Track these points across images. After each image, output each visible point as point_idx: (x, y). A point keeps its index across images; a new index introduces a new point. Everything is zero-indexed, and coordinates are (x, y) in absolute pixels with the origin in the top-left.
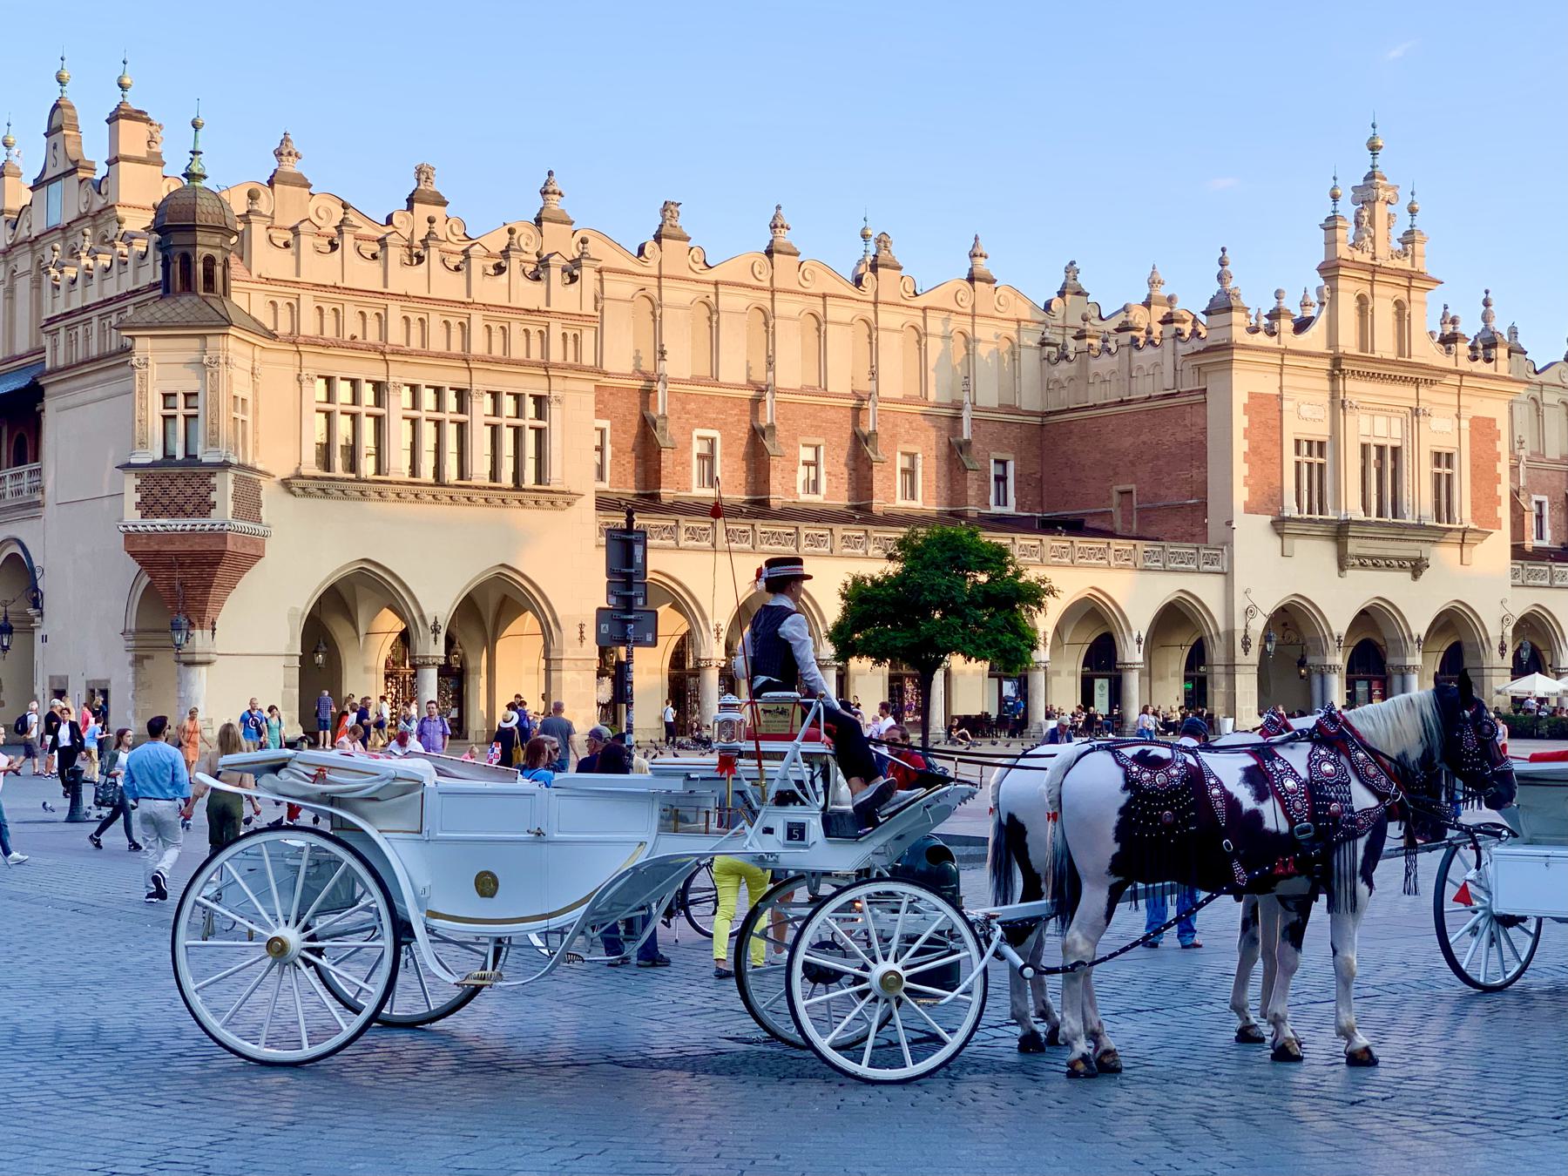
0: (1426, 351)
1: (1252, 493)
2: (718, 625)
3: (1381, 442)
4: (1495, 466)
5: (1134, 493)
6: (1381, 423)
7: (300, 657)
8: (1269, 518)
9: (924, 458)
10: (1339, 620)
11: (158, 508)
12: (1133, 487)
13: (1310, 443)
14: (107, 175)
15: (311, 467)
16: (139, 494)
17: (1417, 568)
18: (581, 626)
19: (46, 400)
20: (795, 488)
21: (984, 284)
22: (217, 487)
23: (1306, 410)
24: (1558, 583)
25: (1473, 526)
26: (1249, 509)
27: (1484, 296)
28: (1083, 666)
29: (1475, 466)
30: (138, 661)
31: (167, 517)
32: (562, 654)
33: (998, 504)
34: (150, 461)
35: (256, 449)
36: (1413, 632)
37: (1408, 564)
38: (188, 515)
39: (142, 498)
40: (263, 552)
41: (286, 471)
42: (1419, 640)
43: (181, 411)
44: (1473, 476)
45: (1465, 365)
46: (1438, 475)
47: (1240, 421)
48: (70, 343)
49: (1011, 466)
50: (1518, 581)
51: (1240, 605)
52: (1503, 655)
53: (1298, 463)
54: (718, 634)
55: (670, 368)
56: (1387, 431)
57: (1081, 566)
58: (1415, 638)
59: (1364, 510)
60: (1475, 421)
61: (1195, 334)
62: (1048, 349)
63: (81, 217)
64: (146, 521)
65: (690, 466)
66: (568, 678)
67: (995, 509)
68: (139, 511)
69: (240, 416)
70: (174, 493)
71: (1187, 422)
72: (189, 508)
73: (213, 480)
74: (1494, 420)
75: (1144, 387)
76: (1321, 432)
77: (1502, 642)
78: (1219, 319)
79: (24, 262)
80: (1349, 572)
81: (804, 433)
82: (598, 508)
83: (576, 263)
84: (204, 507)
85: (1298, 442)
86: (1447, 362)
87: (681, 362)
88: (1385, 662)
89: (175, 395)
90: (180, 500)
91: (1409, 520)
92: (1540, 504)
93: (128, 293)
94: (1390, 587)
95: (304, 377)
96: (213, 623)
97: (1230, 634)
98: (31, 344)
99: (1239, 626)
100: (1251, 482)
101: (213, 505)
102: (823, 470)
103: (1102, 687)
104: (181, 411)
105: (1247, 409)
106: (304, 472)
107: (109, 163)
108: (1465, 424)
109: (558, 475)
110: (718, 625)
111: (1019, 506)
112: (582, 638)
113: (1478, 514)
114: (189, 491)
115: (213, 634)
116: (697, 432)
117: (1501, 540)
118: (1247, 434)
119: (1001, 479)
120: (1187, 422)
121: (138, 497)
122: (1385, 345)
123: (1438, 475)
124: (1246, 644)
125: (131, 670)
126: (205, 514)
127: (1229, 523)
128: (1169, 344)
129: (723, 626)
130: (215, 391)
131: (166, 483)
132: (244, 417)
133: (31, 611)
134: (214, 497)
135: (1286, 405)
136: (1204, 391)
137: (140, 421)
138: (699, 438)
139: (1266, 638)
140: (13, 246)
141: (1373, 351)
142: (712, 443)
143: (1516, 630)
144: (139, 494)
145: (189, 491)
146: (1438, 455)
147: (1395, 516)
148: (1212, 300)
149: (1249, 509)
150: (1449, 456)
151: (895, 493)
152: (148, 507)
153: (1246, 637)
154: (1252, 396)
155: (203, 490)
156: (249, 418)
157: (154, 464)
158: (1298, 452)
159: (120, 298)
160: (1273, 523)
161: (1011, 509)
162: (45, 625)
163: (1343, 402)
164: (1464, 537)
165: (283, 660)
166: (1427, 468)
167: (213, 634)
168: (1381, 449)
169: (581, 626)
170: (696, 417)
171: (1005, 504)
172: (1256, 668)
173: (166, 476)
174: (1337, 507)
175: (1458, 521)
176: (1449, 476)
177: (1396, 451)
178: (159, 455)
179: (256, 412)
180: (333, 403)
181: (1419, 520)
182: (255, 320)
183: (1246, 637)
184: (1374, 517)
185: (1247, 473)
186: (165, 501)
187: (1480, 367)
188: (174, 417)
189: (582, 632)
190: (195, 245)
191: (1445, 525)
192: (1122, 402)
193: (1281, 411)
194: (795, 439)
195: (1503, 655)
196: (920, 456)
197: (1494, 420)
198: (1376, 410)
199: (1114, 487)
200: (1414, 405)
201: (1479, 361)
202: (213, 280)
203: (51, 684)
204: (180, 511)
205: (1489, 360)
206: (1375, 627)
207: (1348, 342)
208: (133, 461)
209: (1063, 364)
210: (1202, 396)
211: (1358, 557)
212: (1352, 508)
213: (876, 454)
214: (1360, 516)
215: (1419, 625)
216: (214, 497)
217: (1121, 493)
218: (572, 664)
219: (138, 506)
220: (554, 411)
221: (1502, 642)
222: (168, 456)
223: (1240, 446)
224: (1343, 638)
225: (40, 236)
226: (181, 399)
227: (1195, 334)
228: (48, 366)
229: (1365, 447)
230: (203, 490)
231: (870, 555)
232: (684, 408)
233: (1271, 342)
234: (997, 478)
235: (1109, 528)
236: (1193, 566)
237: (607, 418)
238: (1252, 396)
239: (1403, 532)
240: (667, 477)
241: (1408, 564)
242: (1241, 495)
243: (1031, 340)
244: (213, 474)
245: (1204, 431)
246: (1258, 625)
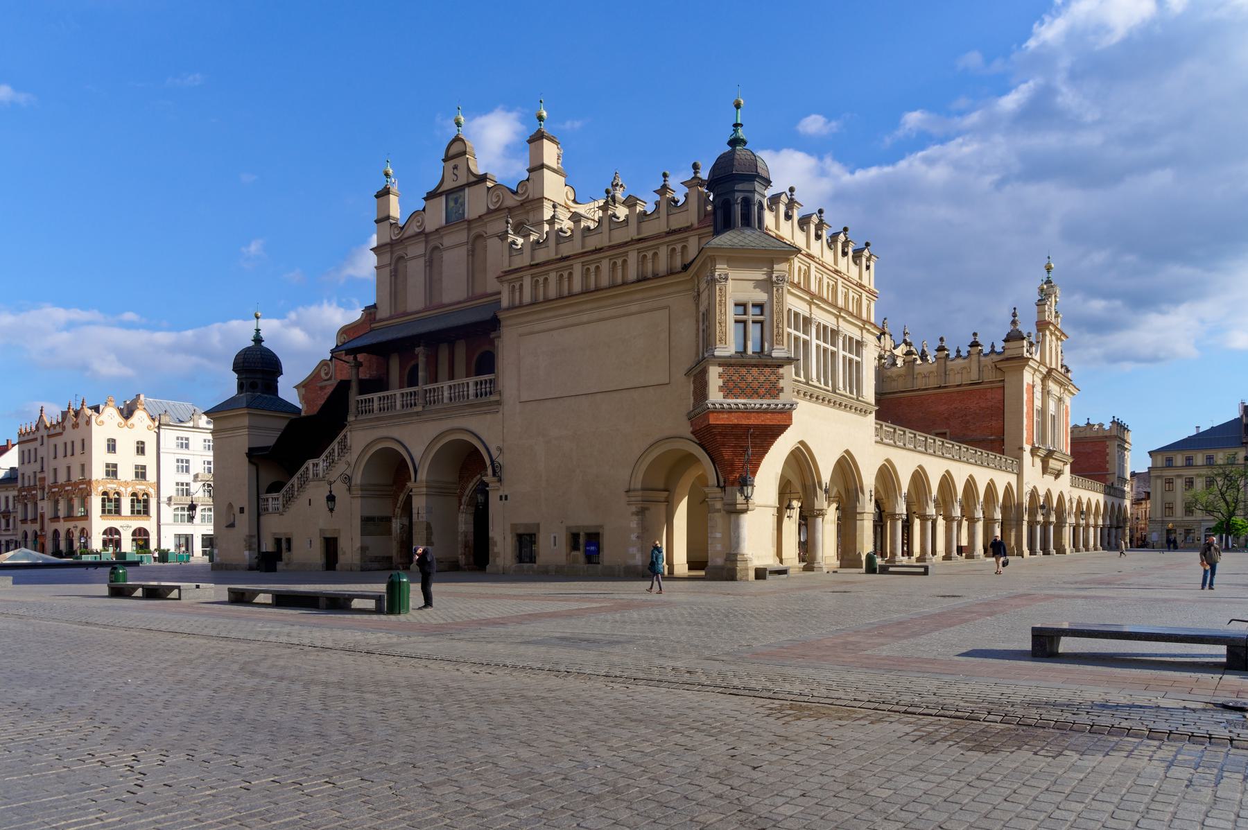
14: (528, 180)
16: (721, 380)
22: (785, 375)
30: (642, 512)
31: (744, 398)
34: (727, 354)
38: (762, 397)
48: (535, 284)
63: (490, 212)
64: (729, 401)
68: (721, 394)
70: (750, 379)
73: (781, 371)
79: (417, 249)
84: (775, 391)
90: (755, 385)
93: (632, 240)
98: (468, 295)
101: (782, 390)
107: (530, 171)
114: (762, 378)
121: (720, 382)
134: (782, 383)
137: (720, 323)
140: (400, 241)
144: (721, 380)
145: (762, 378)
155: (773, 378)
159: (626, 244)
186: (743, 385)
188: (744, 322)
204: (755, 393)
216: (782, 383)
219: (721, 389)
225: (440, 228)
228: (505, 303)
230: (773, 378)
244: (781, 366)
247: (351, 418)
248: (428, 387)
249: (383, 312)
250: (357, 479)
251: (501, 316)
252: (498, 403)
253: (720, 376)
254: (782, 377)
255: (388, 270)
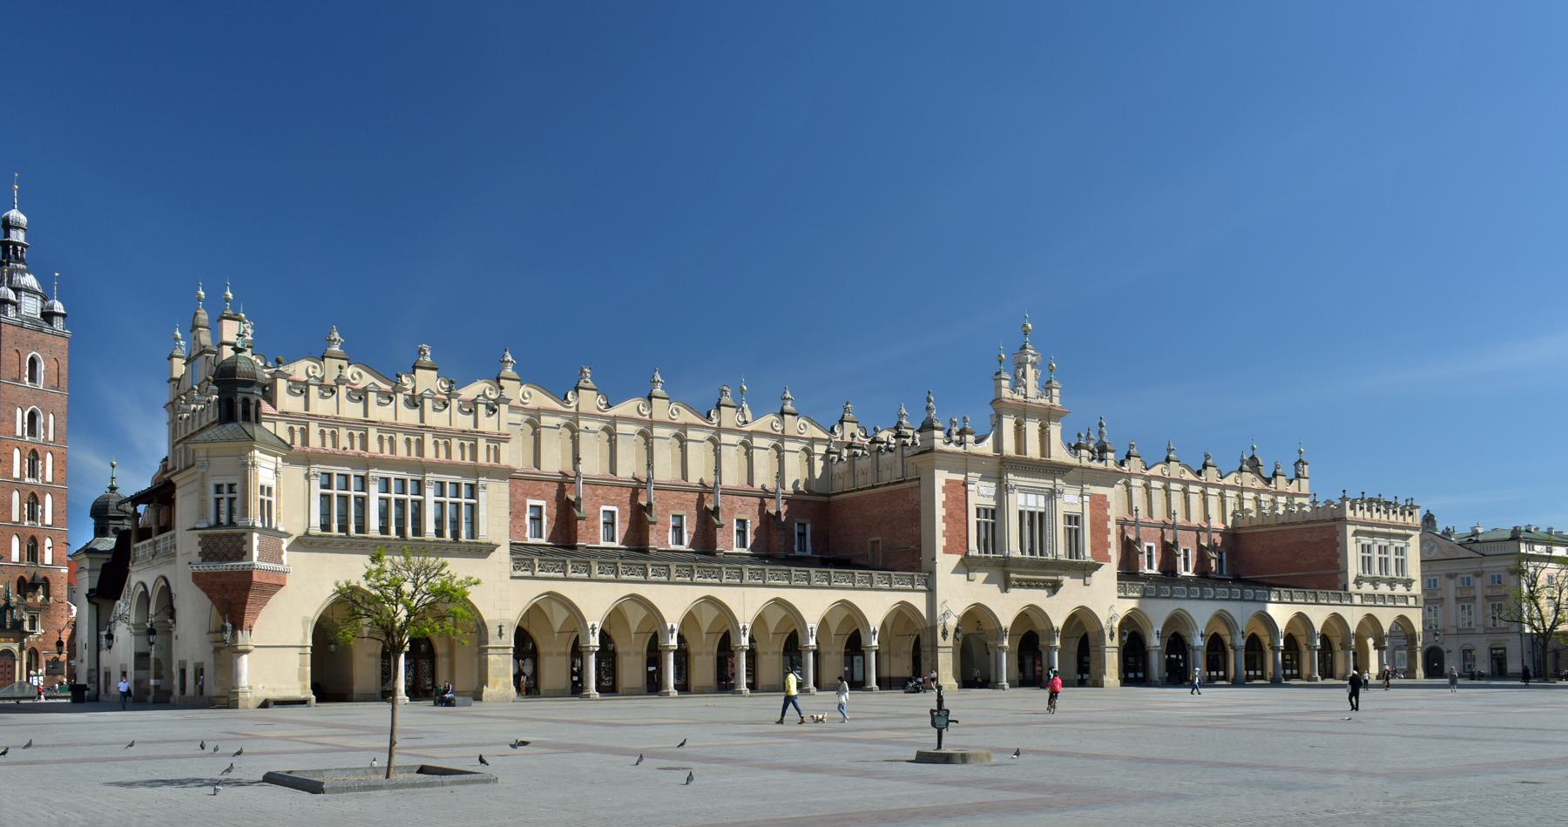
0: (1059, 454)
1: (948, 541)
2: (593, 625)
3: (1032, 509)
4: (1106, 524)
5: (880, 543)
6: (1032, 499)
7: (312, 648)
8: (959, 557)
9: (751, 522)
10: (1006, 621)
11: (212, 555)
12: (879, 538)
13: (986, 510)
15: (316, 530)
16: (200, 547)
17: (1054, 587)
18: (500, 627)
19: (177, 491)
20: (667, 542)
21: (790, 416)
23: (983, 490)
24: (1148, 595)
25: (1092, 560)
26: (947, 550)
27: (1099, 420)
28: (846, 648)
29: (1093, 524)
32: (487, 644)
33: (800, 550)
34: (206, 526)
35: (278, 519)
36: (1054, 625)
37: (1049, 584)
38: (230, 560)
39: (203, 549)
40: (285, 582)
41: (298, 531)
42: (1058, 631)
43: (226, 495)
44: (1092, 530)
45: (1085, 462)
46: (1070, 529)
47: (940, 497)
49: (808, 527)
50: (1123, 594)
51: (940, 612)
52: (1112, 639)
53: (978, 523)
54: (593, 630)
55: (584, 469)
56: (1036, 503)
57: (795, 587)
58: (1055, 629)
59: (1022, 550)
60: (1092, 496)
61: (914, 443)
62: (832, 456)
65: (599, 528)
66: (492, 660)
67: (798, 553)
69: (266, 498)
70: (220, 547)
71: (910, 498)
72: (230, 555)
73: (245, 538)
74: (1105, 496)
75: (886, 477)
76: (991, 503)
77: (1112, 631)
78: (926, 434)
80: (1012, 591)
81: (673, 507)
82: (512, 553)
83: (497, 402)
85: (978, 510)
86: (1073, 461)
87: (665, 470)
88: (1038, 643)
89: (222, 485)
91: (1050, 557)
92: (1150, 549)
94: (1037, 597)
95: (311, 473)
96: (250, 627)
97: (934, 628)
99: (940, 624)
100: (948, 534)
101: (245, 553)
102: (685, 531)
103: (858, 661)
104: (226, 495)
105: (944, 489)
106: (312, 532)
108: (1086, 498)
109: (485, 533)
110: (593, 625)
111: (814, 551)
112: (500, 634)
113: (1096, 553)
114: (230, 545)
115: (250, 633)
116: (604, 508)
117: (1109, 571)
118: (945, 505)
119: (802, 535)
120: (910, 498)
122: (1033, 451)
123: (1070, 529)
124: (945, 634)
125: (212, 656)
126: (240, 559)
127: (934, 559)
128: (899, 450)
129: (597, 626)
130: (245, 481)
131: (216, 540)
132: (269, 498)
133: (170, 621)
135: (970, 487)
136: (919, 479)
138: (604, 511)
139: (957, 630)
141: (1025, 454)
142: (612, 513)
143: (1121, 626)
144: (200, 547)
145: (230, 545)
146: (1070, 517)
147: (1041, 554)
148: (923, 424)
149: (947, 550)
150: (1076, 518)
151: (733, 544)
152: (206, 556)
153: (945, 629)
154: (948, 481)
156: (273, 499)
157: (210, 527)
158: (978, 517)
160: (961, 560)
161: (809, 552)
162: (177, 629)
163: (1006, 485)
164: (1084, 570)
165: (299, 650)
166: (1061, 525)
167: (250, 633)
168: (1032, 514)
169: (500, 627)
170: (603, 498)
171: (805, 550)
172: (951, 650)
173: (216, 535)
174: (1002, 550)
175: (1082, 557)
176: (1076, 530)
177: (1041, 515)
178: (212, 521)
179: (278, 495)
180: (349, 490)
181: (1056, 556)
182: (279, 438)
183: (945, 629)
184: (1027, 555)
185: (945, 529)
187: (1096, 464)
189: (500, 631)
190: (236, 393)
191: (1075, 560)
192: (873, 487)
193: (966, 492)
194: (667, 512)
195: (1112, 639)
196: (749, 521)
197: (1105, 496)
198: (1027, 490)
199: (869, 539)
200: (1051, 486)
201: (1095, 461)
202: (251, 415)
203: (180, 665)
205: (1101, 460)
206: (1080, 623)
207: (1009, 448)
208: (198, 526)
209: (841, 464)
210: (917, 482)
211: (1018, 580)
212: (1014, 550)
213: (718, 519)
214: (1018, 554)
215: (1058, 622)
217: (873, 543)
218: (494, 651)
220: (482, 495)
221: (1112, 631)
222: (218, 524)
223: (940, 512)
224: (1008, 630)
226: (225, 489)
227: (914, 443)
229: (1021, 513)
231: (694, 581)
232: (594, 493)
233: (960, 449)
234: (799, 534)
235: (867, 564)
236: (910, 587)
237: (544, 499)
238: (948, 481)
239: (1045, 566)
240: (581, 535)
241: (1049, 584)
242: (940, 542)
243: (820, 449)
244: (244, 534)
245: (919, 504)
246: (952, 623)
247: (130, 564)
248: (156, 538)
249: (170, 467)
250: (132, 620)
251: (174, 479)
252: (174, 555)
253: (200, 543)
254: (244, 543)
255: (172, 425)
